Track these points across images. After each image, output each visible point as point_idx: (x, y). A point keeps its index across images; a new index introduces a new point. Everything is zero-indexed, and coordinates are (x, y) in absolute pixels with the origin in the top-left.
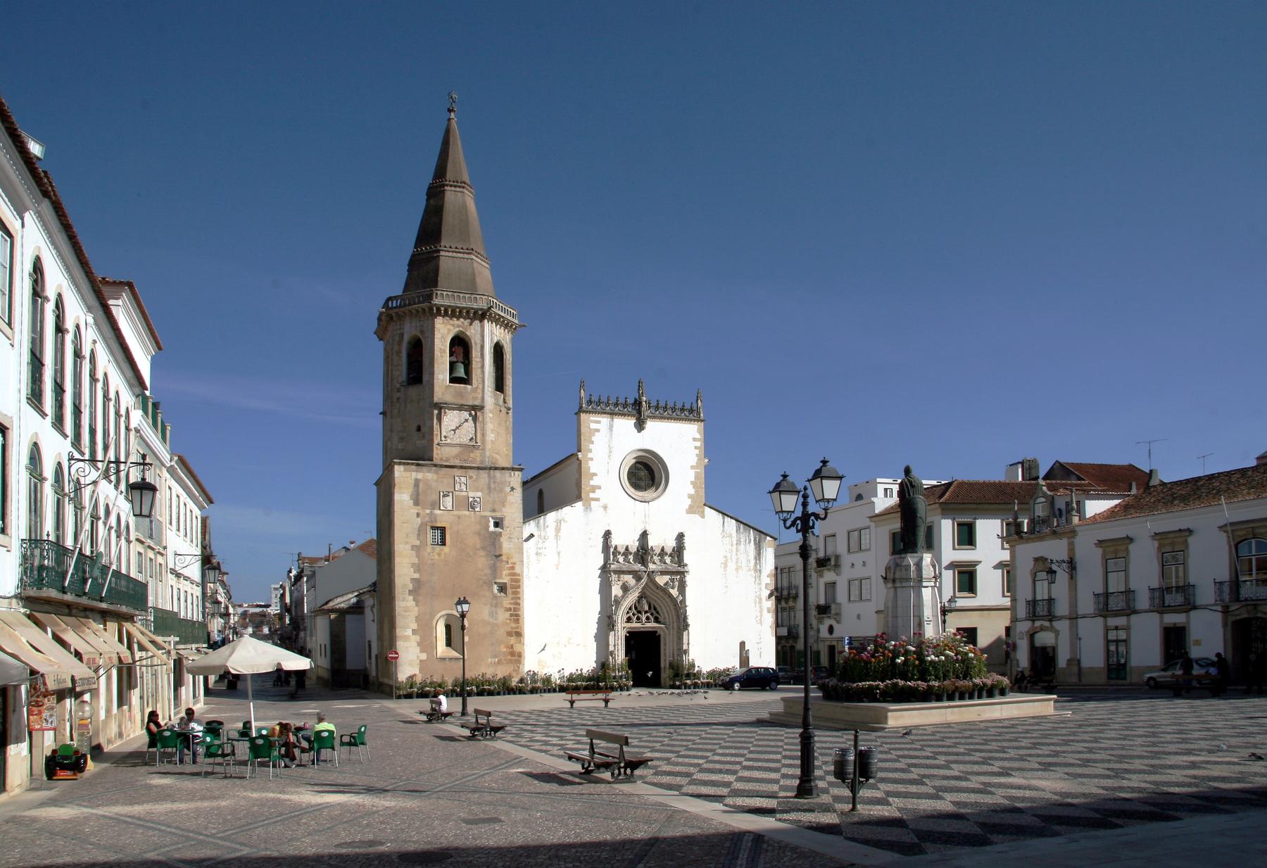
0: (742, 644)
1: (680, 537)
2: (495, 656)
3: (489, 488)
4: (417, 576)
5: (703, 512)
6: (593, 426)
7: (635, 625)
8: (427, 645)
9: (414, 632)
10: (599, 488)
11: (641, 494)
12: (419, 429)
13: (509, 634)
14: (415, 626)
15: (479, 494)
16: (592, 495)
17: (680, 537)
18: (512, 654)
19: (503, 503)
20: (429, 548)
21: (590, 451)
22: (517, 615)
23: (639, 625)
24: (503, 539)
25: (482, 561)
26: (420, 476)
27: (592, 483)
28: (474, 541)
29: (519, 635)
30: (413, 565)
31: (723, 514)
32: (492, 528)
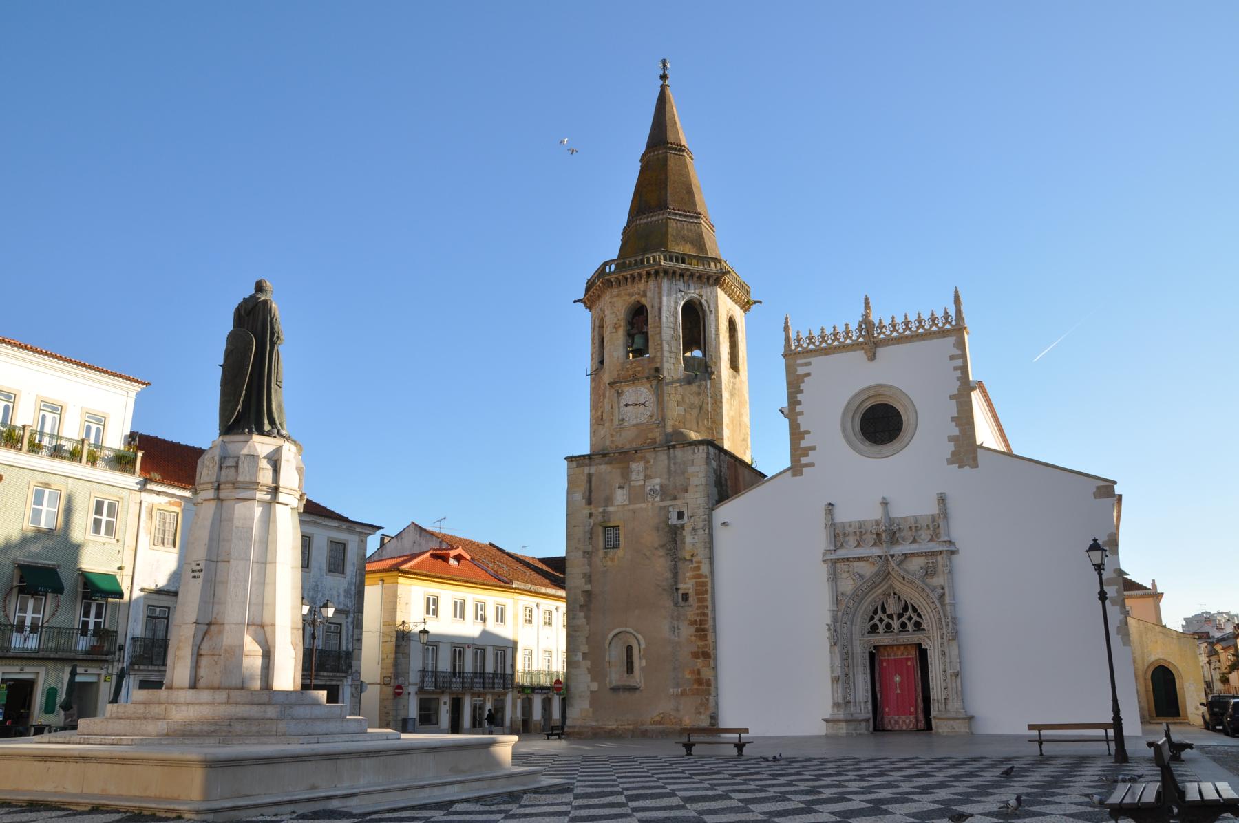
1: (942, 499)
2: (678, 685)
4: (588, 587)
5: (975, 459)
8: (597, 673)
9: (585, 656)
10: (814, 448)
13: (696, 655)
14: (585, 649)
15: (658, 481)
16: (804, 460)
17: (942, 499)
18: (699, 682)
21: (799, 403)
22: (704, 630)
25: (661, 564)
26: (593, 470)
27: (803, 444)
28: (652, 539)
29: (707, 655)
30: (585, 574)
32: (673, 520)
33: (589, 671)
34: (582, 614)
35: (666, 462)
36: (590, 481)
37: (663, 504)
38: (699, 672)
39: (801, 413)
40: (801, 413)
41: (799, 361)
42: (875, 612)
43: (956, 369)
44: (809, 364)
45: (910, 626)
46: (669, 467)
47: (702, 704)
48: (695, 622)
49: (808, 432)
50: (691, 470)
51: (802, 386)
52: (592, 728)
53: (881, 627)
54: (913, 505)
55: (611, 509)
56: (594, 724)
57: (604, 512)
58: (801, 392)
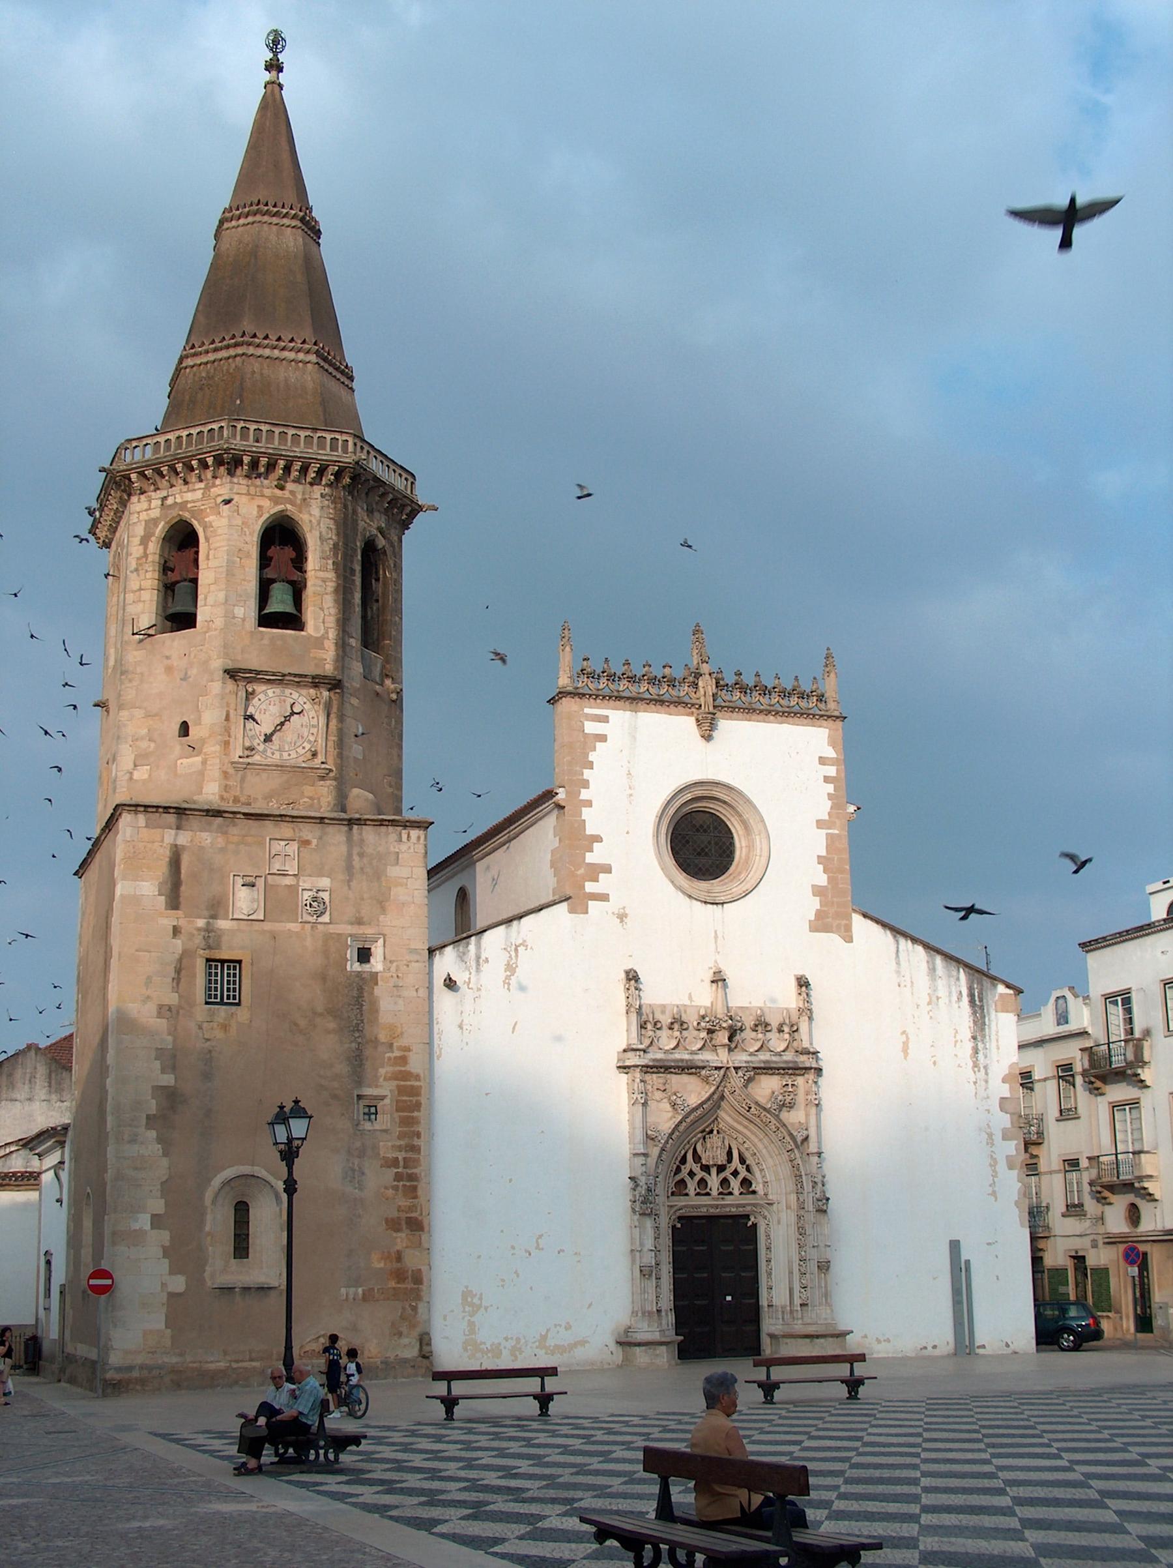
0: (955, 1246)
2: (357, 1283)
3: (349, 868)
4: (168, 1080)
5: (848, 928)
6: (591, 727)
7: (694, 1203)
8: (184, 1255)
9: (157, 1221)
10: (607, 869)
11: (704, 885)
12: (184, 729)
13: (394, 1225)
14: (157, 1205)
15: (325, 882)
16: (590, 887)
17: (803, 983)
18: (400, 1275)
19: (382, 903)
20: (201, 1011)
21: (586, 784)
22: (412, 1178)
23: (705, 1200)
24: (381, 991)
26: (183, 838)
27: (590, 858)
31: (897, 932)
33: (166, 1252)
34: (153, 1134)
35: (344, 849)
36: (175, 863)
37: (332, 929)
38: (399, 1257)
39: (589, 803)
40: (589, 803)
41: (587, 710)
42: (683, 1160)
43: (827, 779)
44: (605, 719)
45: (735, 1184)
46: (350, 856)
47: (402, 1318)
48: (395, 1162)
49: (598, 839)
50: (393, 872)
51: (592, 757)
52: (174, 1370)
53: (692, 1186)
54: (761, 989)
55: (222, 924)
56: (174, 1360)
57: (208, 929)
58: (590, 765)
